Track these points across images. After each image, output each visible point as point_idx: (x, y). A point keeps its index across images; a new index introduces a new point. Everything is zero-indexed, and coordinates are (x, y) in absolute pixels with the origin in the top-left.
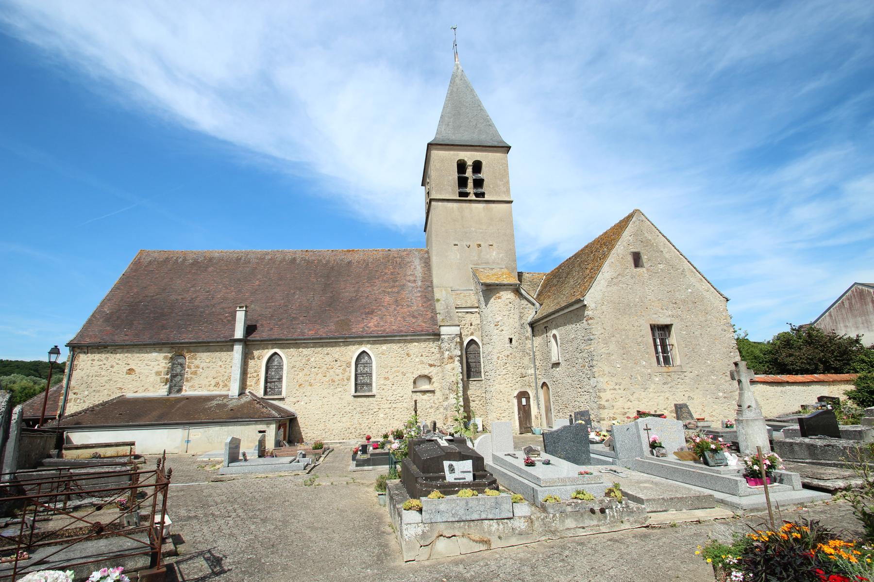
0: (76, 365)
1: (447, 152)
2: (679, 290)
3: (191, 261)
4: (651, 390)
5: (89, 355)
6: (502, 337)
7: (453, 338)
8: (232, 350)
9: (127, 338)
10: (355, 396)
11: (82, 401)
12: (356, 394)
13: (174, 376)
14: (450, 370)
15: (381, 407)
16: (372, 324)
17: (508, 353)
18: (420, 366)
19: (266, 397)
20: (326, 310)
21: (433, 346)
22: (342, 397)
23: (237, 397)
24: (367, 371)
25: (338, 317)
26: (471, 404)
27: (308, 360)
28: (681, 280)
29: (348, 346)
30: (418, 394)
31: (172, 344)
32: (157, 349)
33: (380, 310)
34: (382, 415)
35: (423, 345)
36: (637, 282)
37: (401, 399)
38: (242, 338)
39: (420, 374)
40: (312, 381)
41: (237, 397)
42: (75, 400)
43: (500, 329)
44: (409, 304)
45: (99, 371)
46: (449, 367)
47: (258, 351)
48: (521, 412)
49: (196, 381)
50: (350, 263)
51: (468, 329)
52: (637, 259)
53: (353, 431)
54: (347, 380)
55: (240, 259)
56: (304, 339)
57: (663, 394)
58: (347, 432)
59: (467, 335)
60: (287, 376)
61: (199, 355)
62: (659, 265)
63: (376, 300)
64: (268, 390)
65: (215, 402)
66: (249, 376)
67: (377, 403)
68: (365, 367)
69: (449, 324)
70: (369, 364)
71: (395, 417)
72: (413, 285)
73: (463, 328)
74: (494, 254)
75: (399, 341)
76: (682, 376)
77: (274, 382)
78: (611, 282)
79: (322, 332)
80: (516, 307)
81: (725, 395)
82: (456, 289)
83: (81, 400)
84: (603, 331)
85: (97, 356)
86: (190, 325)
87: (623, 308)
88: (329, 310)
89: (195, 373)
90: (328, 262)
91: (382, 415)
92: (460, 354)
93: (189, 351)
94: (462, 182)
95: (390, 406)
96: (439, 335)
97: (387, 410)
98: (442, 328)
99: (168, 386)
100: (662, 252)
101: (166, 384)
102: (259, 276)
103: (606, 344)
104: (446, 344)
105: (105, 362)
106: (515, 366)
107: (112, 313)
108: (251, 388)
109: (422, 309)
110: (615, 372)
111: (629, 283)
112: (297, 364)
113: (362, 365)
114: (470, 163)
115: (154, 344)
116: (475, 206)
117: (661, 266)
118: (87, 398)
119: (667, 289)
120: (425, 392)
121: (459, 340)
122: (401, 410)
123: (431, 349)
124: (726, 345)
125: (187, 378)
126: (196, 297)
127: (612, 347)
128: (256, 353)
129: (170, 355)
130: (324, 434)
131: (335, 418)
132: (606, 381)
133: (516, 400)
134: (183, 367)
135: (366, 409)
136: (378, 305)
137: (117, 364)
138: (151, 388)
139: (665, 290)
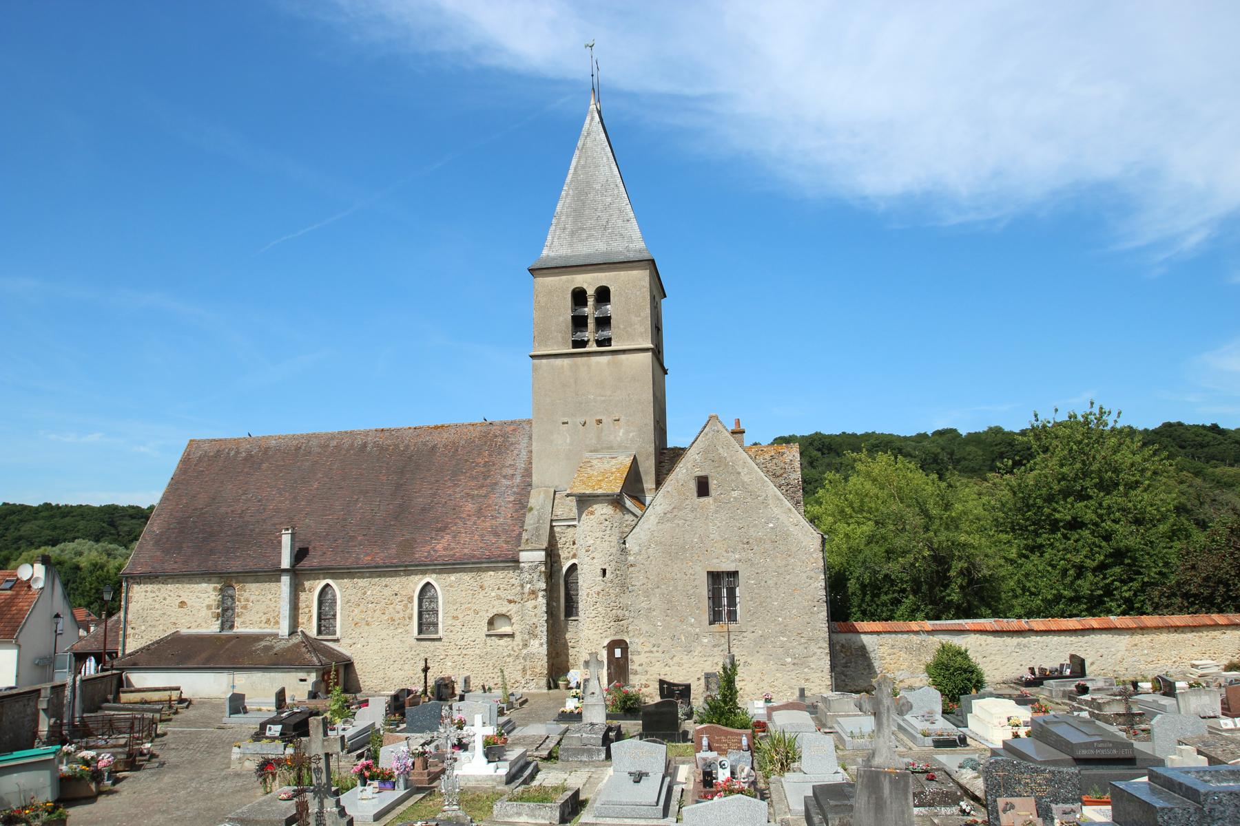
0: (131, 597)
1: (557, 278)
2: (755, 525)
3: (244, 454)
4: (696, 654)
5: (142, 585)
6: (592, 567)
7: (538, 566)
8: (279, 581)
9: (176, 566)
10: (418, 640)
11: (140, 637)
12: (422, 636)
13: (225, 610)
14: (531, 609)
15: (448, 654)
16: (441, 546)
17: (599, 588)
18: (496, 603)
19: (320, 637)
20: (391, 525)
21: (512, 577)
22: (403, 639)
23: (287, 637)
24: (433, 608)
25: (403, 535)
26: (570, 651)
27: (365, 593)
28: (761, 511)
29: (410, 575)
30: (493, 638)
31: (220, 573)
32: (206, 579)
33: (455, 524)
34: (449, 664)
35: (501, 574)
36: (698, 516)
37: (472, 643)
38: (288, 567)
39: (496, 613)
40: (369, 619)
41: (287, 637)
42: (134, 635)
43: (591, 556)
44: (495, 513)
45: (153, 603)
46: (530, 604)
47: (309, 582)
48: (612, 667)
49: (247, 616)
50: (434, 447)
51: (569, 549)
52: (703, 487)
53: (416, 681)
54: (409, 618)
55: (300, 448)
56: (358, 568)
57: (711, 658)
58: (409, 682)
59: (567, 558)
60: (341, 613)
61: (248, 586)
62: (733, 492)
63: (454, 509)
64: (323, 628)
65: (263, 643)
66: (300, 612)
67: (444, 648)
68: (431, 602)
69: (530, 548)
70: (434, 599)
71: (466, 666)
72: (509, 483)
73: (563, 548)
74: (621, 434)
75: (471, 570)
76: (740, 637)
77: (329, 619)
78: (662, 519)
79: (379, 560)
80: (615, 525)
81: (796, 661)
82: (562, 489)
83: (139, 635)
84: (645, 581)
85: (150, 587)
86: (238, 548)
87: (675, 551)
88: (394, 525)
89: (245, 607)
90: (407, 447)
91: (449, 664)
92: (545, 588)
93: (238, 582)
94: (579, 322)
95: (459, 653)
96: (517, 561)
97: (456, 657)
98: (521, 553)
99: (220, 622)
100: (739, 473)
101: (218, 620)
102: (320, 475)
103: (648, 597)
104: (526, 574)
105: (157, 593)
106: (608, 606)
107: (162, 534)
108: (304, 626)
109: (509, 521)
110: (654, 632)
111: (688, 518)
112: (352, 598)
113: (429, 600)
114: (591, 291)
115: (202, 574)
116: (595, 360)
117: (735, 494)
118: (145, 633)
119: (738, 525)
120: (501, 636)
121: (543, 569)
122: (472, 658)
123: (511, 581)
124: (809, 597)
125: (238, 613)
126: (247, 509)
127: (655, 600)
128: (307, 584)
129: (219, 586)
130: (383, 683)
131: (395, 665)
132: (642, 641)
133: (606, 652)
134: (233, 600)
135: (431, 656)
136: (455, 516)
137: (170, 596)
138: (203, 624)
139: (736, 526)
